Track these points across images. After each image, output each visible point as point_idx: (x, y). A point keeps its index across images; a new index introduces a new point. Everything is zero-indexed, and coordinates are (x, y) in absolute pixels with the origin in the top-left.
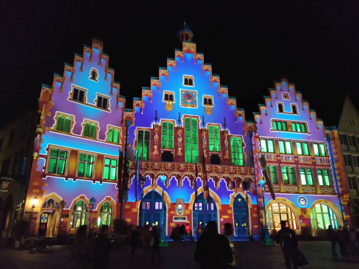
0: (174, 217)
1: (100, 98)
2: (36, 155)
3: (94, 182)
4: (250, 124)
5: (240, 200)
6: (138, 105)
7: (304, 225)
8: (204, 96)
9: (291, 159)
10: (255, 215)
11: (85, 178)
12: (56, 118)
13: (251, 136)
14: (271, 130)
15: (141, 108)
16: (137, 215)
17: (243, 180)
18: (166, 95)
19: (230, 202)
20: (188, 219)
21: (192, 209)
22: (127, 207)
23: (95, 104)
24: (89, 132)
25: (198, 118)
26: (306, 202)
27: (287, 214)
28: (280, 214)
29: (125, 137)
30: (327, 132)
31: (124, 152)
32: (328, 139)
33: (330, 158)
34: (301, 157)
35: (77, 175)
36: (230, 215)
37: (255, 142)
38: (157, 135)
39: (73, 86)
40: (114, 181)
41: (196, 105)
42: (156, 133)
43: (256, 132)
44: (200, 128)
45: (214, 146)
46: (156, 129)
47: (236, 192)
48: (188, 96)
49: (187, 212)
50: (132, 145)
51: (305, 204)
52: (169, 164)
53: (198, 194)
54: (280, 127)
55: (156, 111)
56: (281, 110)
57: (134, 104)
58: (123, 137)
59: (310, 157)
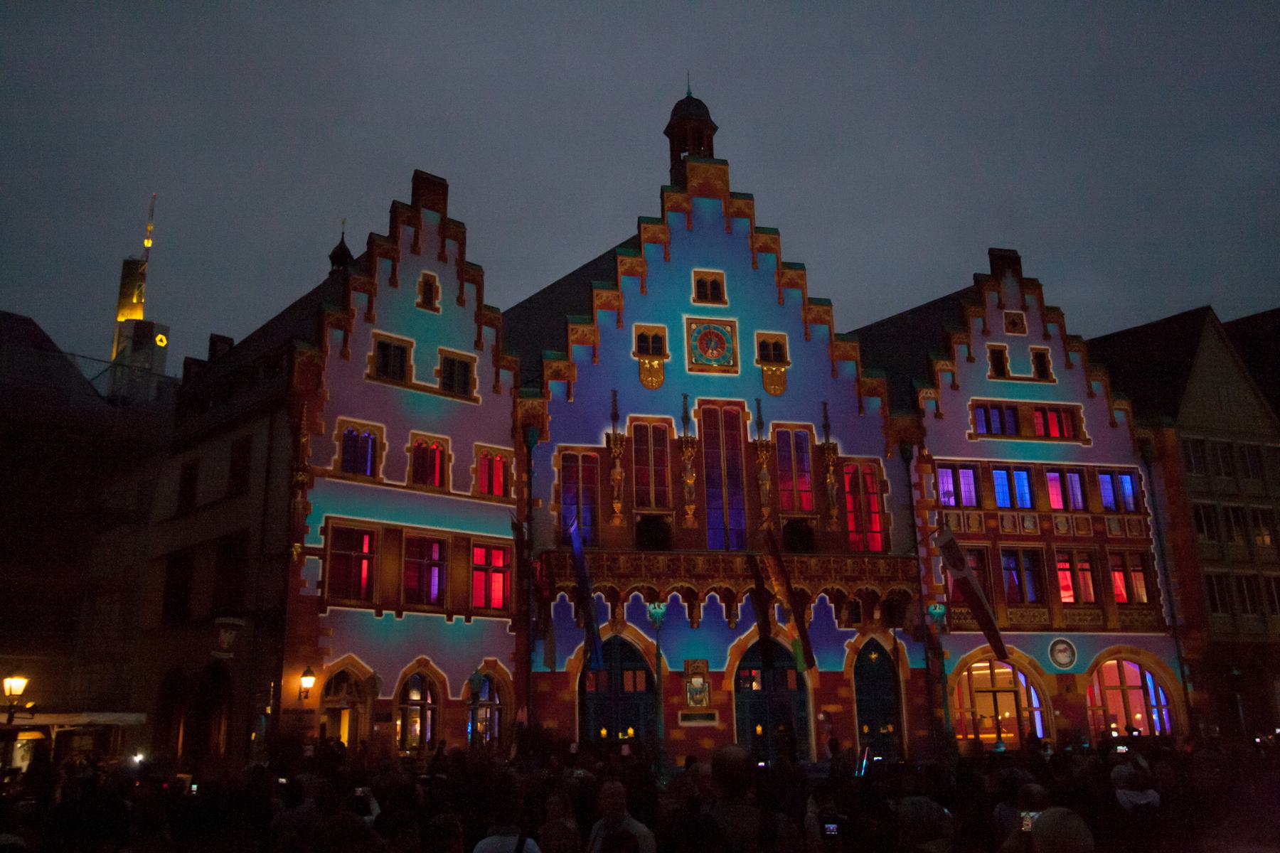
0: (680, 713)
3: (450, 619)
4: (904, 420)
6: (557, 375)
7: (1065, 723)
8: (759, 335)
9: (1028, 524)
10: (920, 700)
12: (338, 437)
13: (907, 459)
14: (970, 436)
15: (569, 383)
16: (574, 709)
17: (884, 597)
18: (642, 338)
19: (841, 662)
20: (723, 719)
21: (732, 687)
24: (427, 468)
25: (743, 409)
26: (1073, 654)
27: (1016, 694)
28: (994, 693)
29: (525, 477)
30: (1145, 433)
31: (525, 525)
32: (1146, 462)
33: (1149, 519)
34: (1061, 518)
36: (845, 702)
37: (921, 478)
38: (618, 469)
39: (375, 335)
40: (504, 610)
41: (735, 364)
42: (618, 462)
43: (921, 448)
44: (750, 440)
46: (617, 450)
48: (710, 338)
49: (720, 697)
50: (547, 500)
51: (1071, 662)
52: (662, 559)
54: (996, 425)
55: (615, 393)
56: (999, 369)
57: (547, 373)
58: (519, 476)
59: (1089, 516)
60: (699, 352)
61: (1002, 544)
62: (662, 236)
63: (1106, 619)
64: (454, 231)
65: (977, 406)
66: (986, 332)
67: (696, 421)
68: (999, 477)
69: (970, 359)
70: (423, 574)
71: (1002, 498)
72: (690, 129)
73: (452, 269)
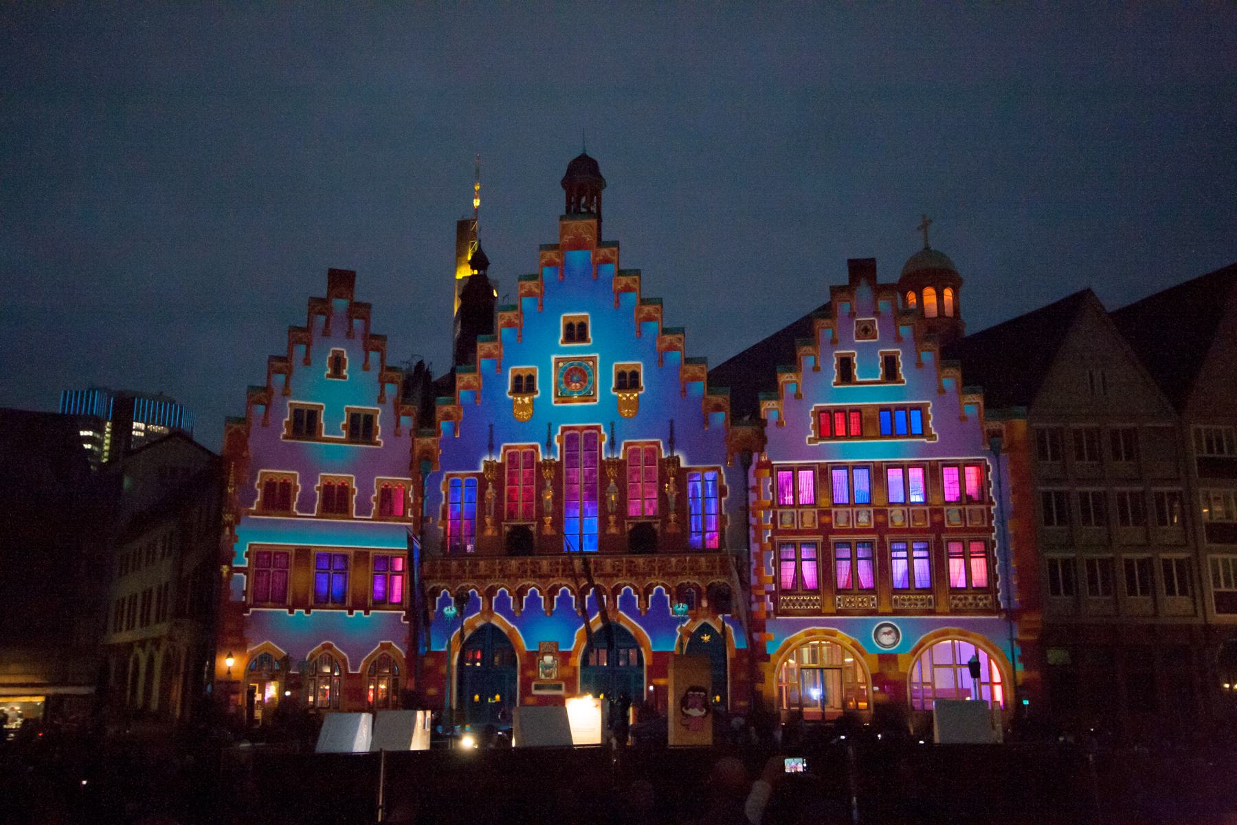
1: (354, 417)
2: (225, 569)
3: (351, 613)
4: (745, 431)
5: (706, 638)
6: (448, 417)
9: (863, 519)
10: (742, 676)
11: (330, 605)
12: (259, 486)
13: (746, 467)
18: (518, 379)
22: (429, 662)
24: (335, 501)
26: (898, 636)
30: (995, 425)
32: (995, 452)
33: (992, 508)
37: (758, 481)
39: (291, 405)
40: (399, 606)
41: (595, 394)
43: (761, 451)
47: (694, 620)
48: (576, 373)
49: (567, 672)
50: (435, 519)
51: (894, 644)
55: (491, 426)
57: (439, 415)
58: (415, 499)
59: (927, 508)
60: (563, 386)
61: (833, 538)
62: (537, 291)
63: (937, 603)
64: (360, 310)
65: (820, 412)
66: (834, 342)
67: (558, 445)
68: (839, 476)
69: (816, 369)
70: (334, 580)
71: (841, 495)
72: (583, 183)
73: (358, 341)
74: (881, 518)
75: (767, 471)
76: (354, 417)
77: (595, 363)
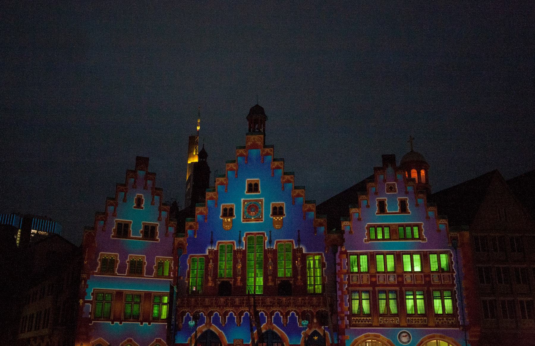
1: (146, 227)
2: (81, 301)
3: (142, 324)
5: (316, 338)
6: (191, 227)
9: (392, 279)
11: (132, 320)
12: (100, 260)
15: (195, 231)
18: (225, 210)
23: (140, 235)
24: (136, 269)
32: (455, 248)
33: (454, 274)
35: (122, 318)
37: (341, 260)
39: (116, 221)
43: (342, 246)
44: (266, 248)
45: (284, 270)
47: (310, 329)
48: (253, 207)
51: (409, 342)
53: (264, 331)
57: (187, 227)
58: (175, 268)
60: (247, 214)
61: (377, 289)
62: (235, 168)
64: (150, 176)
66: (376, 193)
67: (244, 242)
72: (257, 118)
74: (400, 279)
75: (345, 256)
76: (146, 227)
77: (262, 204)
